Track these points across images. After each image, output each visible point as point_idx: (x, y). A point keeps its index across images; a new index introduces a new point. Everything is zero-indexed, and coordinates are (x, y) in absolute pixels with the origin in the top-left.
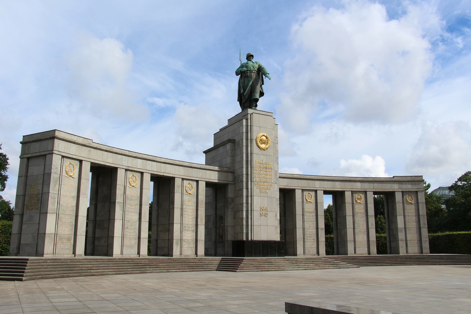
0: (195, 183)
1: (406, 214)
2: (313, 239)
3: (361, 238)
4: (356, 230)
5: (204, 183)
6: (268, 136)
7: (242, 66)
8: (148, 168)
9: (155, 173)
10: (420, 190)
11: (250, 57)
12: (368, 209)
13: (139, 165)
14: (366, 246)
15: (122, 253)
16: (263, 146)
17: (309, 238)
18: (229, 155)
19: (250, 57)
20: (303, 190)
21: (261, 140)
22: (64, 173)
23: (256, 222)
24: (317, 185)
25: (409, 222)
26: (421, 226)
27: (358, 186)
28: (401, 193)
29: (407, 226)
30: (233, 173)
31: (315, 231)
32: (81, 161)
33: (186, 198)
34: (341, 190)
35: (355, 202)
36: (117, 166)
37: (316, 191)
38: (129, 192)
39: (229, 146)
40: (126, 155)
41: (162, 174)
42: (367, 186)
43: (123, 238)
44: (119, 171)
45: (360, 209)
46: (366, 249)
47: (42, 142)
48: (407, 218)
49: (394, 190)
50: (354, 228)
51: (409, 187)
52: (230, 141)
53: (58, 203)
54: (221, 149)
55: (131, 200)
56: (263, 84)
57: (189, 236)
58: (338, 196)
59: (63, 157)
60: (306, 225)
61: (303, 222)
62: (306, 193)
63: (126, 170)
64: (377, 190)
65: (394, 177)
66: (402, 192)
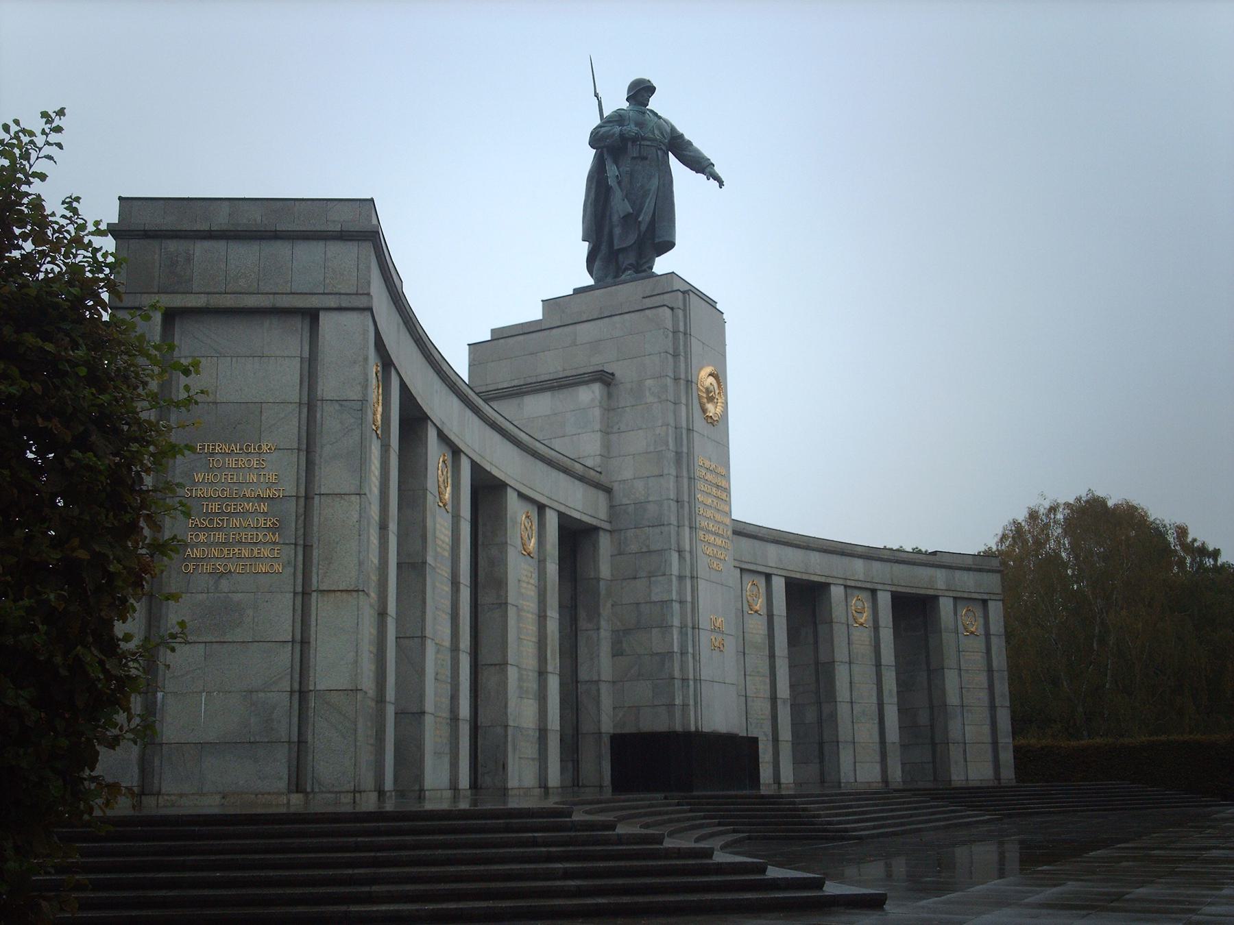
10: (993, 597)
18: (597, 427)
23: (705, 674)
27: (858, 568)
30: (608, 491)
31: (767, 706)
34: (823, 580)
35: (851, 621)
37: (768, 577)
46: (878, 767)
47: (282, 249)
51: (968, 582)
64: (900, 589)
65: (935, 553)
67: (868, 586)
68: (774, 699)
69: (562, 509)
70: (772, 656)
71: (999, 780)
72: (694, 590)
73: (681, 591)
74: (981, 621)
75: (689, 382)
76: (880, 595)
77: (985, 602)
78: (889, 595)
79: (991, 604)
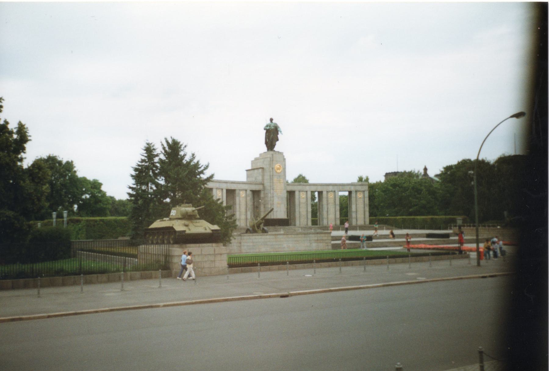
3: (332, 216)
4: (329, 213)
7: (267, 126)
11: (271, 120)
16: (278, 171)
19: (271, 120)
20: (299, 191)
27: (331, 188)
33: (241, 199)
39: (260, 170)
42: (335, 188)
45: (331, 201)
50: (327, 212)
52: (261, 168)
54: (256, 171)
57: (243, 217)
58: (320, 193)
60: (301, 210)
62: (301, 193)
75: (273, 168)
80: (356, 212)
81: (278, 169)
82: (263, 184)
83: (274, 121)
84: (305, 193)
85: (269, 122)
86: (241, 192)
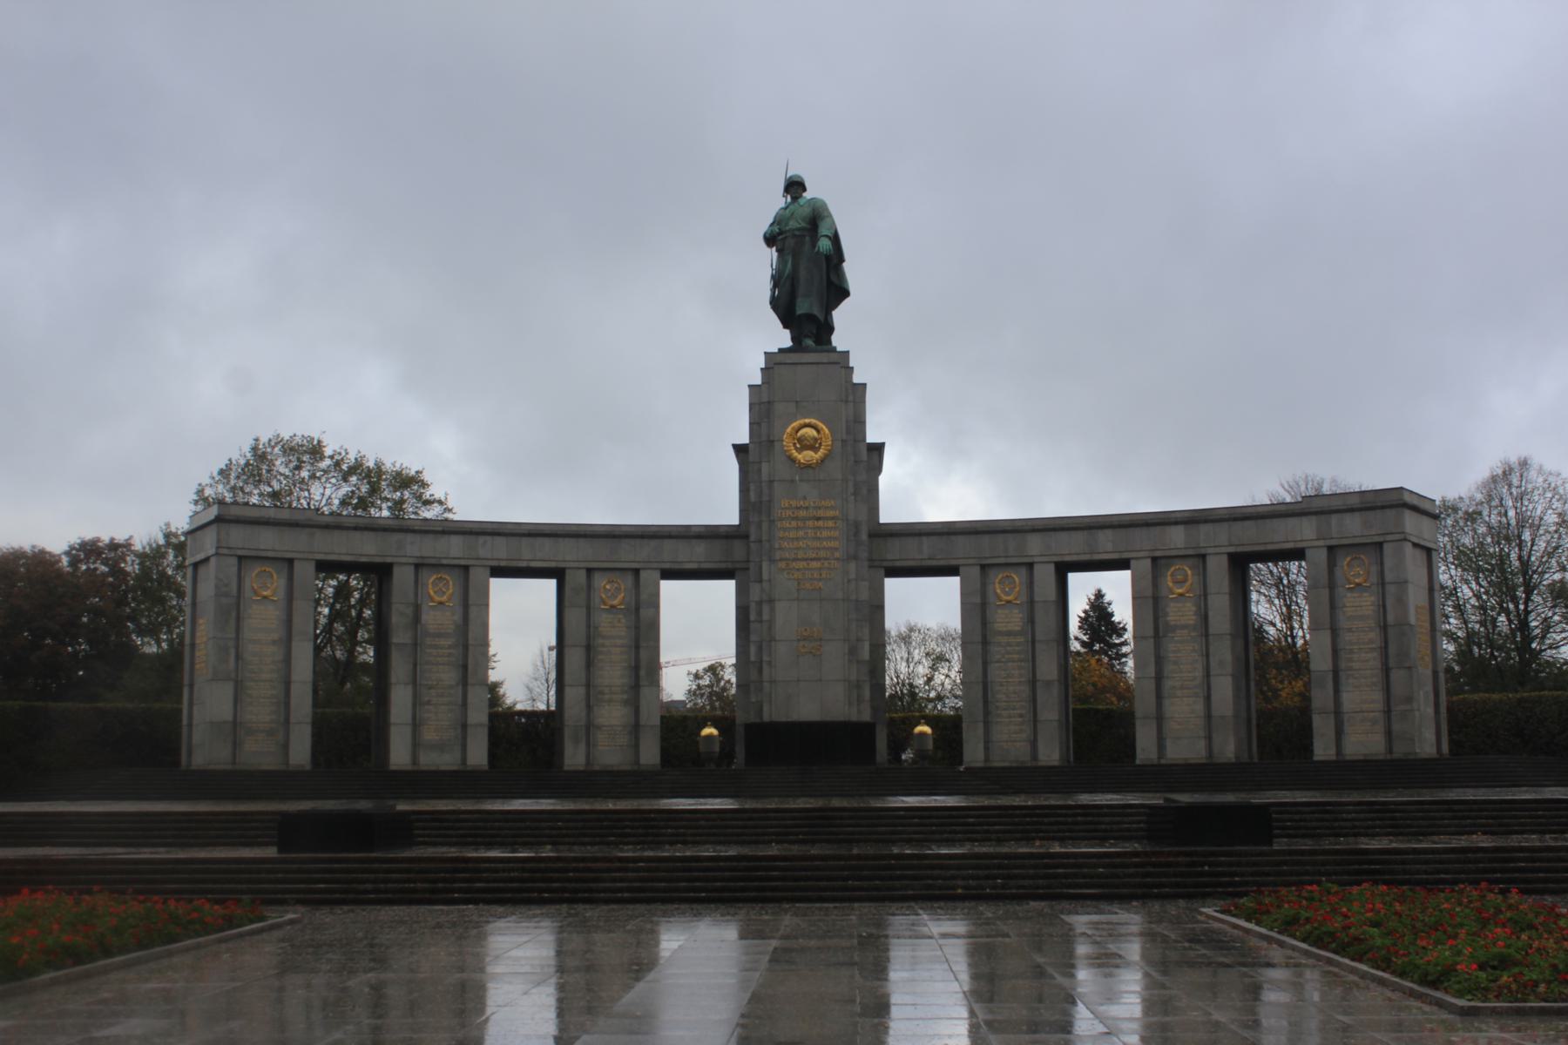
0: (630, 578)
1: (1343, 623)
2: (1021, 716)
4: (1168, 684)
5: (658, 574)
6: (821, 425)
8: (482, 553)
9: (503, 564)
10: (1389, 538)
11: (794, 187)
12: (1211, 614)
13: (454, 548)
14: (1202, 733)
15: (415, 760)
17: (1004, 713)
19: (794, 187)
21: (799, 440)
22: (248, 593)
24: (1034, 546)
25: (1351, 652)
26: (1392, 663)
27: (1177, 538)
28: (1323, 554)
29: (1343, 665)
32: (290, 561)
33: (604, 621)
36: (389, 560)
38: (430, 618)
40: (414, 531)
41: (524, 564)
43: (416, 725)
44: (396, 571)
45: (1181, 613)
46: (1202, 744)
48: (1346, 638)
49: (1300, 545)
51: (1353, 527)
53: (238, 657)
55: (439, 635)
56: (842, 260)
57: (612, 715)
59: (240, 558)
60: (996, 673)
61: (985, 664)
62: (997, 577)
63: (417, 566)
64: (1240, 549)
66: (1331, 549)
67: (1190, 552)
68: (1033, 682)
69: (667, 566)
70: (1033, 642)
71: (1391, 752)
72: (772, 610)
73: (760, 613)
74: (1374, 569)
76: (1212, 562)
77: (1380, 545)
78: (1224, 561)
79: (1387, 548)
80: (1336, 673)
81: (804, 445)
82: (747, 537)
83: (807, 195)
84: (1018, 577)
85: (779, 201)
86: (601, 581)
